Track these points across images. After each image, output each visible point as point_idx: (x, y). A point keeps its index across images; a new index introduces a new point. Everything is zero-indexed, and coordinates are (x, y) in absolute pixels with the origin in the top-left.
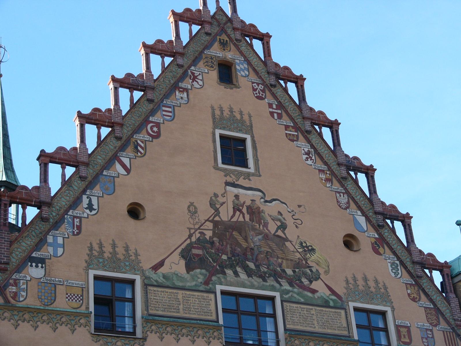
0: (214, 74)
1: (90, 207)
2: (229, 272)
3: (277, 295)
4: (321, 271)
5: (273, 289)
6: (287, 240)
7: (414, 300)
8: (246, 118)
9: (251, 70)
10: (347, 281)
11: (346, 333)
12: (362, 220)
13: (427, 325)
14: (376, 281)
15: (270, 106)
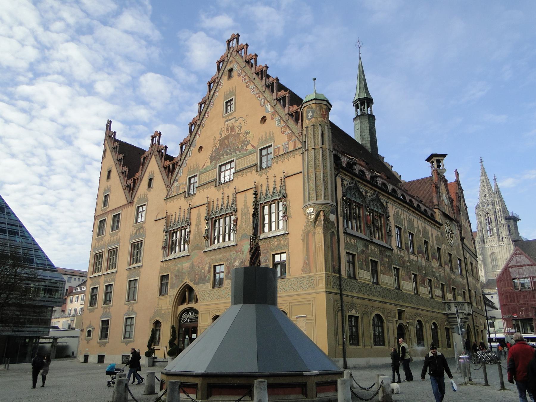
0: (227, 77)
1: (190, 155)
2: (222, 157)
3: (234, 158)
4: (251, 140)
5: (234, 157)
6: (241, 133)
7: (283, 133)
8: (234, 89)
9: (238, 66)
10: (259, 139)
11: (255, 162)
12: (269, 107)
13: (287, 142)
14: (270, 133)
15: (243, 77)
